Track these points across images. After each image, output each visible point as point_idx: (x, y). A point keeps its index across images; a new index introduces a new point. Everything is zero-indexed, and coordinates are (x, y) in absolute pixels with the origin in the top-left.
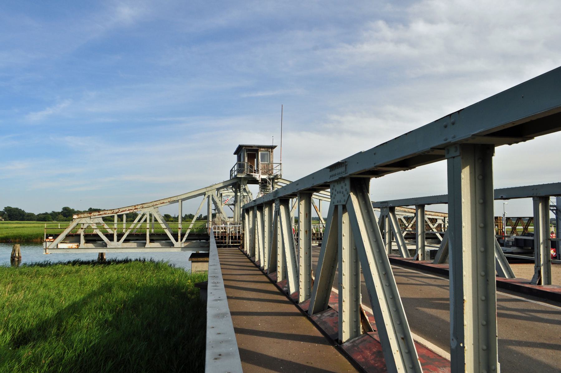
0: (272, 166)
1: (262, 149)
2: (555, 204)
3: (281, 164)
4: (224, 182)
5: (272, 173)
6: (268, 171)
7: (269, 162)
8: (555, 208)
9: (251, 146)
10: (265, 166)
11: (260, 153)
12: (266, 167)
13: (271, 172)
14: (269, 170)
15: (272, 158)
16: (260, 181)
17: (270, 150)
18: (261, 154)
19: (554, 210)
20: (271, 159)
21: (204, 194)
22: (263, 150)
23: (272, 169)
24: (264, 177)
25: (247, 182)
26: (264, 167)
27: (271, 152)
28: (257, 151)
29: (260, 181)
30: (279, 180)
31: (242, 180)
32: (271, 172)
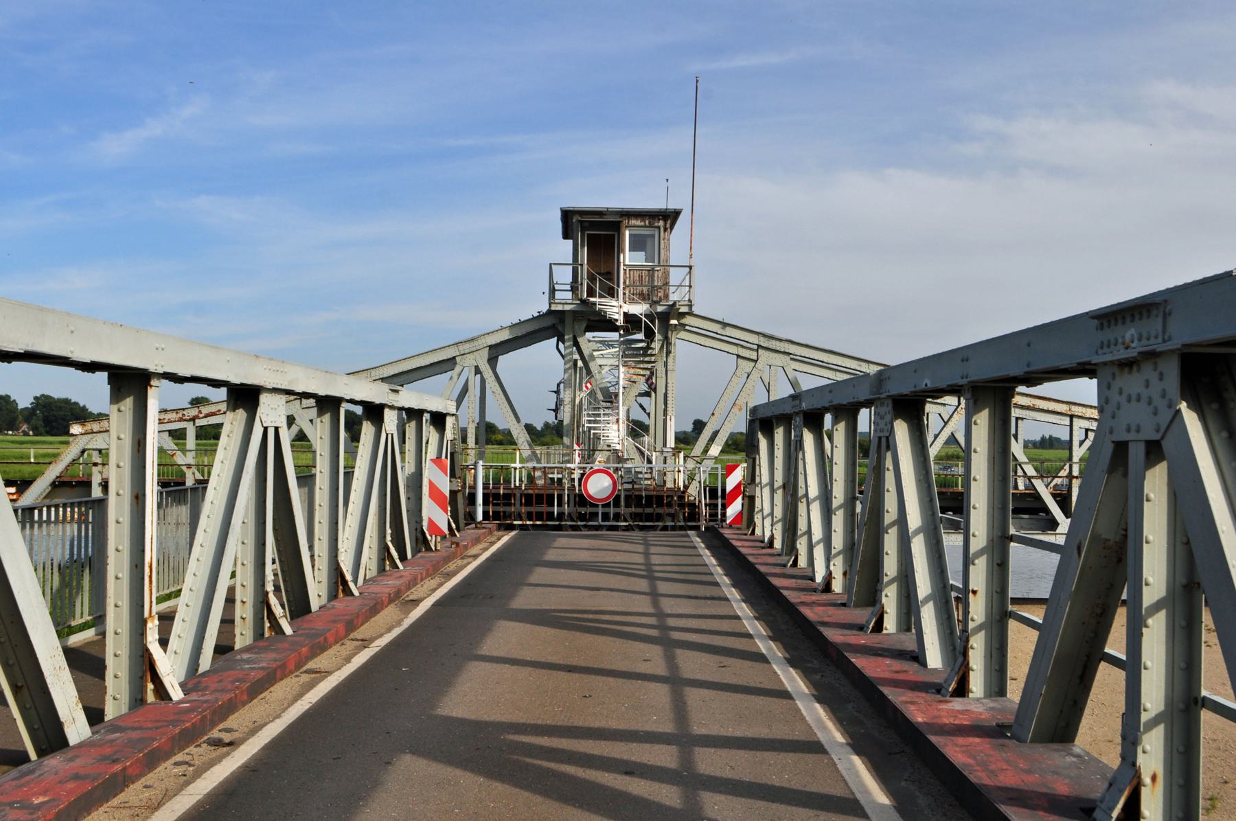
0: (666, 275)
1: (633, 222)
3: (690, 267)
4: (513, 326)
5: (667, 296)
7: (656, 263)
11: (627, 233)
12: (646, 279)
13: (661, 294)
14: (653, 288)
15: (668, 248)
16: (620, 322)
17: (661, 223)
18: (630, 235)
20: (662, 251)
22: (638, 223)
23: (666, 284)
24: (639, 309)
25: (584, 325)
26: (641, 277)
27: (662, 229)
28: (616, 227)
29: (620, 322)
30: (688, 320)
31: (568, 320)
32: (661, 294)
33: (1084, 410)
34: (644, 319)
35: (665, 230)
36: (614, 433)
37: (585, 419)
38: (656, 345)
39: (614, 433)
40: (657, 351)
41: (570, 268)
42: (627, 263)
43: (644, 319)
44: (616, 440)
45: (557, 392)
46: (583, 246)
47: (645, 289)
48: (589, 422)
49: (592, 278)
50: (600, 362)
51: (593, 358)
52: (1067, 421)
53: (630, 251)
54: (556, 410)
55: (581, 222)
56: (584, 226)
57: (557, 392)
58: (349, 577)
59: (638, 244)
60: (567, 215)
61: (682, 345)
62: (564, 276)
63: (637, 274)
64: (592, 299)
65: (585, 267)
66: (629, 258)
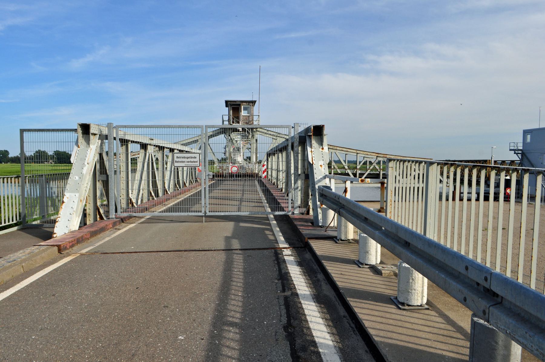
0: (253, 118)
1: (244, 104)
2: (521, 148)
3: (259, 116)
6: (249, 120)
8: (520, 152)
9: (235, 102)
10: (247, 117)
11: (242, 107)
12: (247, 119)
13: (251, 123)
14: (250, 121)
15: (253, 110)
17: (251, 104)
19: (520, 153)
21: (196, 141)
22: (245, 104)
23: (253, 120)
24: (246, 126)
26: (246, 118)
28: (240, 105)
32: (251, 123)
33: (360, 152)
34: (247, 129)
35: (252, 106)
36: (240, 159)
37: (232, 155)
38: (250, 136)
39: (240, 159)
40: (250, 138)
41: (228, 116)
42: (243, 115)
43: (247, 129)
44: (240, 161)
45: (225, 148)
46: (231, 110)
47: (247, 121)
48: (233, 156)
49: (233, 119)
50: (236, 139)
51: (234, 139)
52: (356, 154)
53: (243, 110)
54: (225, 153)
55: (230, 104)
56: (231, 105)
57: (225, 148)
58: (167, 190)
59: (245, 109)
60: (227, 102)
61: (258, 136)
62: (226, 118)
63: (245, 117)
64: (233, 124)
65: (232, 116)
66: (243, 113)
